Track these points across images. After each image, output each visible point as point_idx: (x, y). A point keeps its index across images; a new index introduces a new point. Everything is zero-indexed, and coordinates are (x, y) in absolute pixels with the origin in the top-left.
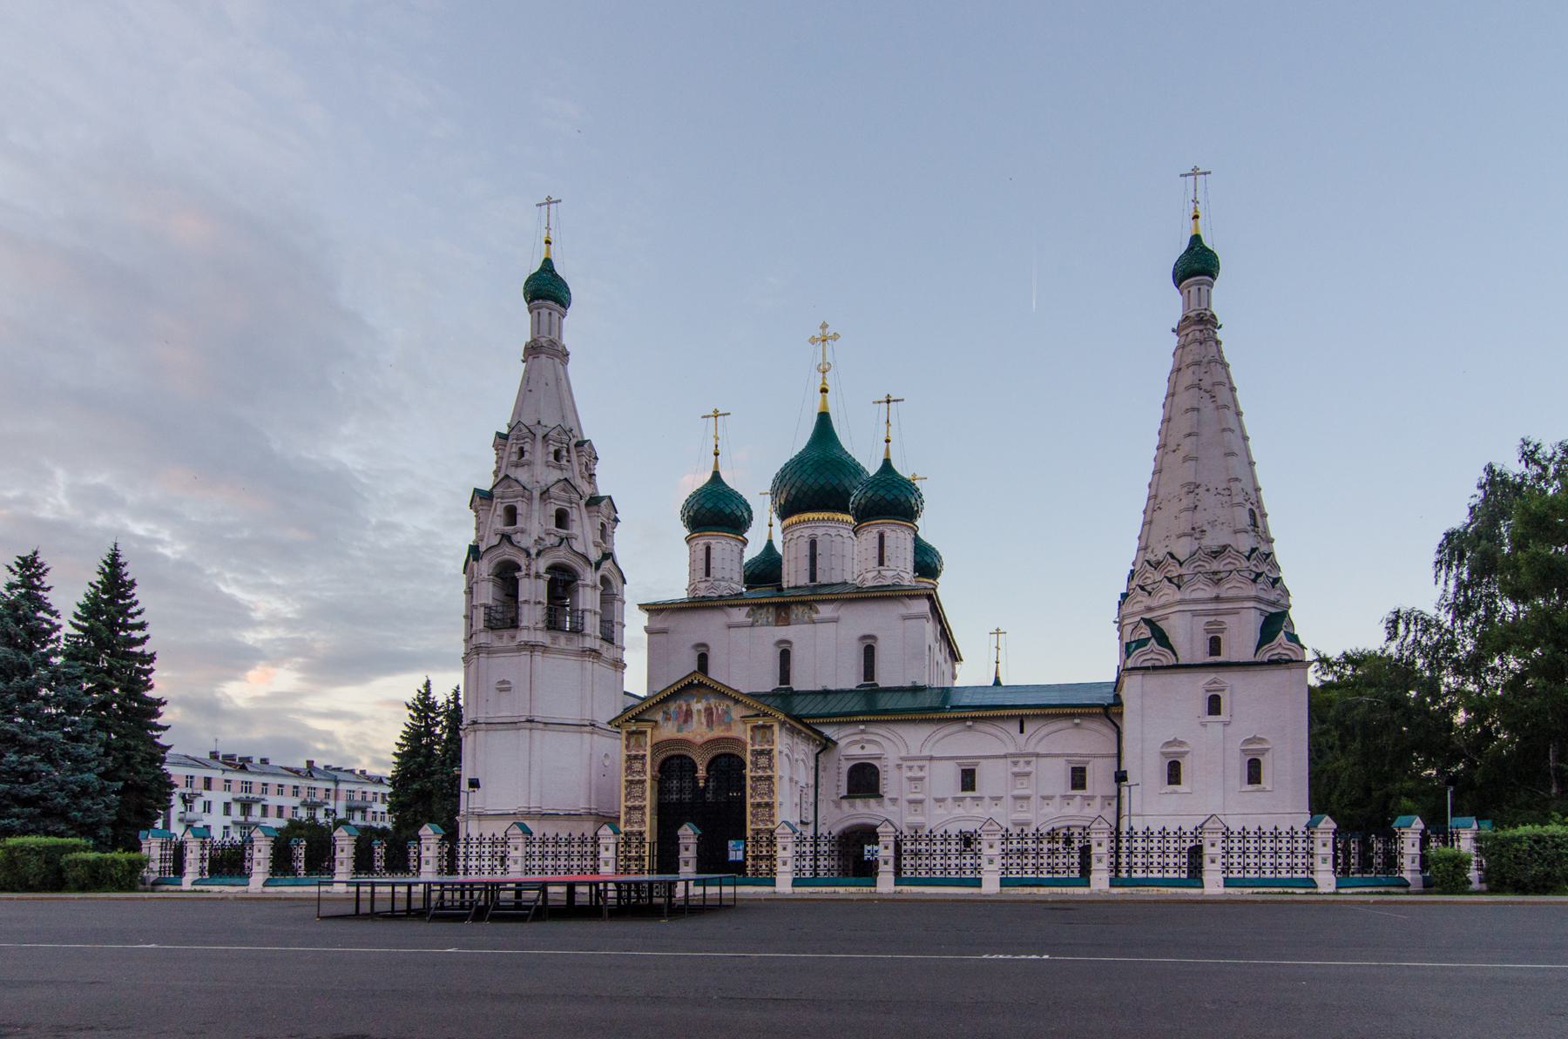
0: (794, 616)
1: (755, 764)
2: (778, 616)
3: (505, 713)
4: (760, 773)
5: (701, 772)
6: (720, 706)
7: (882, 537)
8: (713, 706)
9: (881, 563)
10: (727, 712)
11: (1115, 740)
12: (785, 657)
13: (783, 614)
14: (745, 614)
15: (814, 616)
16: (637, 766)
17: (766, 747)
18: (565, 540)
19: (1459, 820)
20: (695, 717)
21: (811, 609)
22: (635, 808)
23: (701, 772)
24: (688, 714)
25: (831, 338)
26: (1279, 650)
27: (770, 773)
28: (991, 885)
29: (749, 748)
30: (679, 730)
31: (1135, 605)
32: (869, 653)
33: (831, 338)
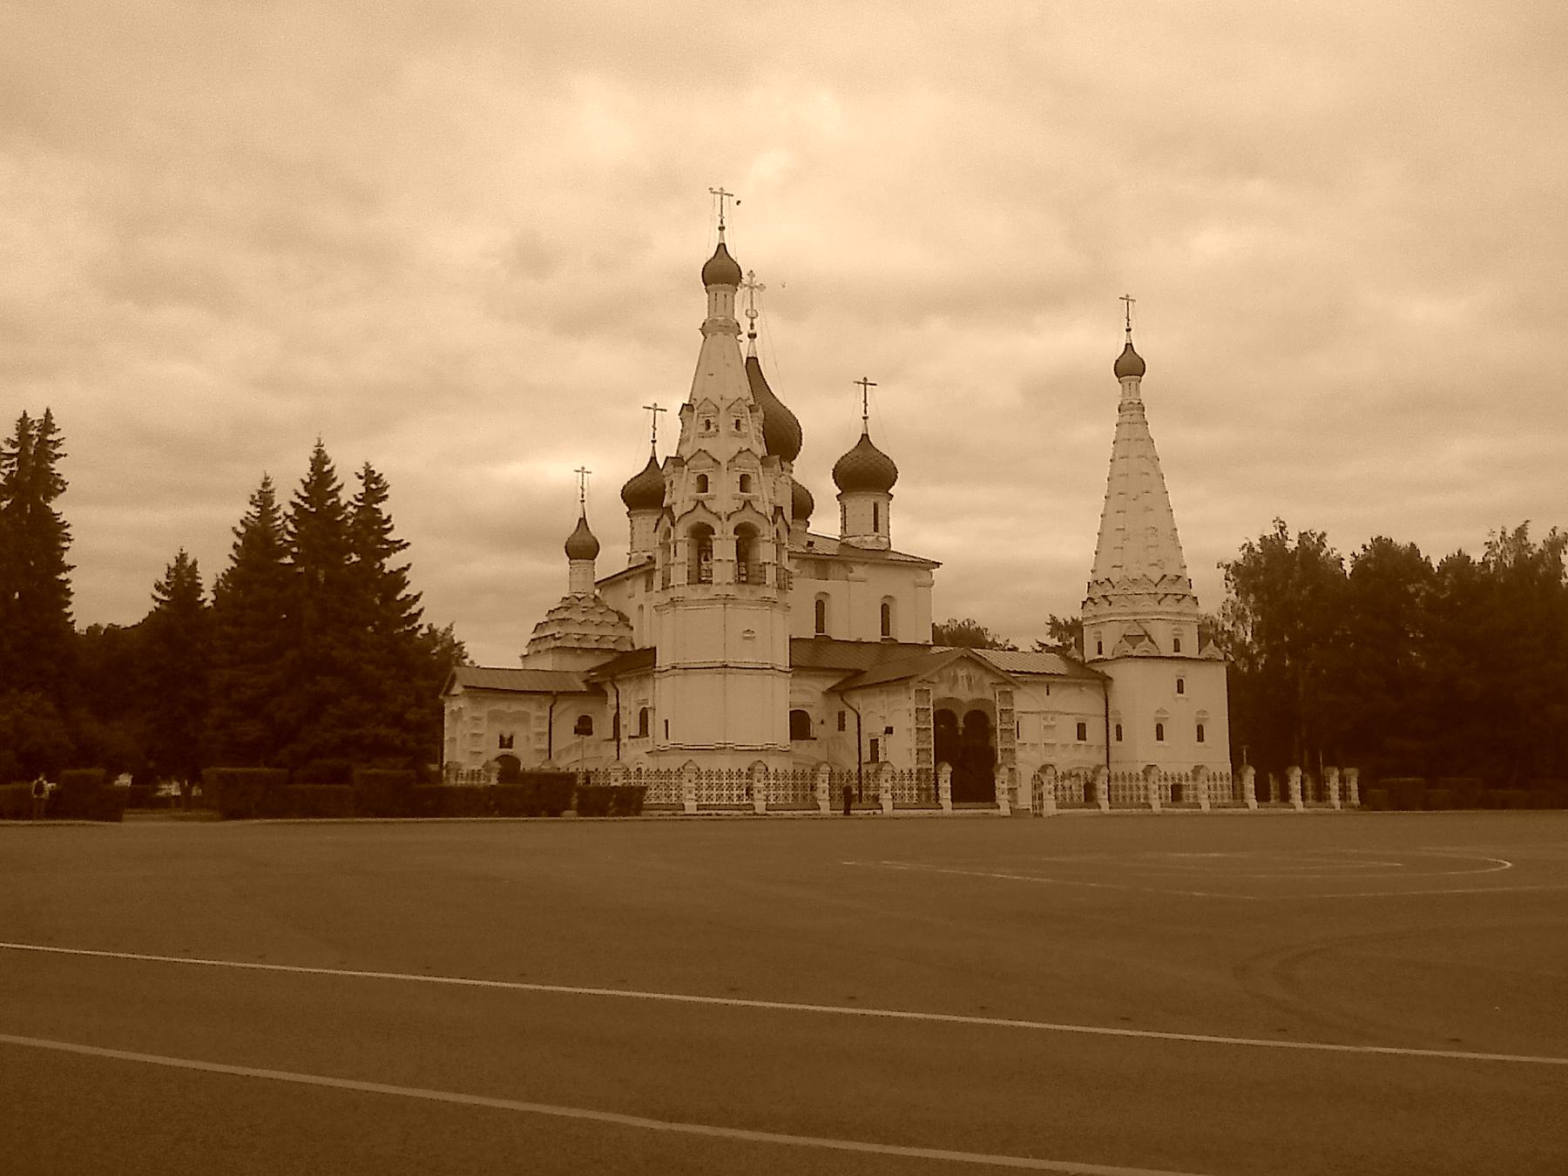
0: (831, 571)
1: (1001, 720)
2: (816, 569)
3: (749, 659)
4: (1005, 727)
5: (961, 724)
6: (977, 674)
7: (876, 506)
8: (972, 674)
9: (876, 530)
10: (981, 678)
11: (1104, 702)
12: (820, 606)
13: (819, 568)
14: (794, 565)
15: (851, 575)
16: (922, 718)
17: (1009, 708)
18: (748, 503)
19: (1329, 769)
20: (960, 679)
21: (845, 565)
22: (923, 750)
23: (961, 724)
24: (955, 678)
25: (751, 279)
26: (1210, 652)
27: (1010, 727)
28: (1206, 807)
29: (998, 708)
30: (951, 690)
31: (1123, 608)
32: (885, 609)
33: (751, 279)
